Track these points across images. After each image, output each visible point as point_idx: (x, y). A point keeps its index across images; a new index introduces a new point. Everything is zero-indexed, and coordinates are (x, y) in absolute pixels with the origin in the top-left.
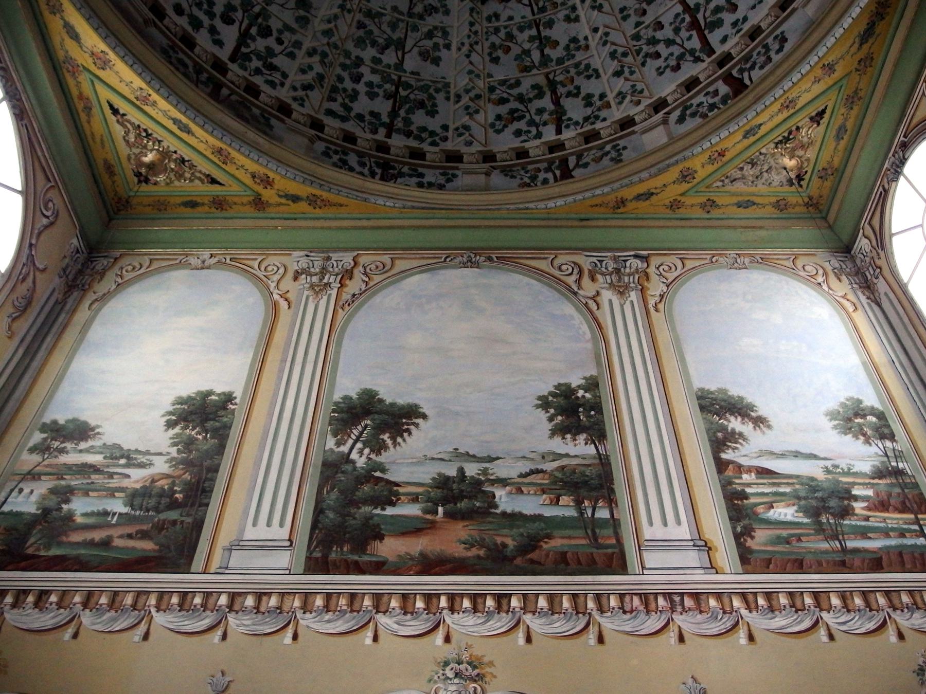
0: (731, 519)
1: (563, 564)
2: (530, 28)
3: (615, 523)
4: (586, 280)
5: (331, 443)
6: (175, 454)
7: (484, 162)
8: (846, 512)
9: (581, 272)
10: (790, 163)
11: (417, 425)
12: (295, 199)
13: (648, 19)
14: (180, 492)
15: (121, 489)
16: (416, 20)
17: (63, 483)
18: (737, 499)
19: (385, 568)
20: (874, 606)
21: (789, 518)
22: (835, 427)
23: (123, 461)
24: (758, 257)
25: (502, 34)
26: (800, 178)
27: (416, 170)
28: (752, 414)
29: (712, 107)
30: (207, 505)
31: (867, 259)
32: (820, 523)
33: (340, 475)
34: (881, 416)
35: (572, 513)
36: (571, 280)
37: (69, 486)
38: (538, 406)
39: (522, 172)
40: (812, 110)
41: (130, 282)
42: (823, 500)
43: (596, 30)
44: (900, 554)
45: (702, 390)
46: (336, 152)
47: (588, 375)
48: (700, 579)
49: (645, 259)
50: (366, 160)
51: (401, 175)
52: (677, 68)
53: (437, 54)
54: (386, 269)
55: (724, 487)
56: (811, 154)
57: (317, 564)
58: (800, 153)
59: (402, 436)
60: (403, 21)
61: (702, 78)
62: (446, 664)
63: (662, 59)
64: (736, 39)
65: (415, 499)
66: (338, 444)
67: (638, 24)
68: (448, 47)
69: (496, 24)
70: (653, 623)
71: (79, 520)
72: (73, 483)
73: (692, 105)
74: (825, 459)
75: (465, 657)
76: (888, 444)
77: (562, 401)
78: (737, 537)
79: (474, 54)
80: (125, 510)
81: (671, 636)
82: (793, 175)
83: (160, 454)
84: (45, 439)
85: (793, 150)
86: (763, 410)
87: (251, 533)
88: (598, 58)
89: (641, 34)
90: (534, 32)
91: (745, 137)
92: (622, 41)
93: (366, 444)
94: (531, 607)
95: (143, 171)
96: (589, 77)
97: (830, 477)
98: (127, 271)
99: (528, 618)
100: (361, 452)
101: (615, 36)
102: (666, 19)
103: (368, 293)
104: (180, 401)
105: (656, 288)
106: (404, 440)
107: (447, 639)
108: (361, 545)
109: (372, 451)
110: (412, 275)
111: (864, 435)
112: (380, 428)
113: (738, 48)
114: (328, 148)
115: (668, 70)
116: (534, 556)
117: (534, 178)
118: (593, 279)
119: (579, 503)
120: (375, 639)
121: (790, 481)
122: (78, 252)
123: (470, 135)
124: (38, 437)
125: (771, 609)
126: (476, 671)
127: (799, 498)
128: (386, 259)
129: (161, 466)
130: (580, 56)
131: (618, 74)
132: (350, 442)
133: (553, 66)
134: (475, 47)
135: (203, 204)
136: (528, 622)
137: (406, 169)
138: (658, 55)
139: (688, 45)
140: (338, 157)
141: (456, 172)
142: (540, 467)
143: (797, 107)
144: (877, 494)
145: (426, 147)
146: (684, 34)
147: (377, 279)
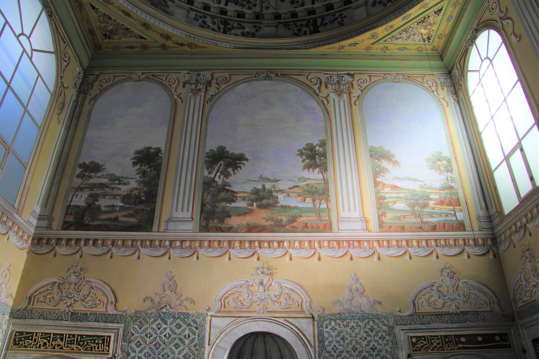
0: (377, 208)
1: (306, 228)
3: (328, 210)
4: (323, 88)
5: (206, 173)
6: (139, 179)
7: (275, 19)
8: (425, 206)
9: (321, 83)
10: (423, 31)
11: (244, 164)
12: (182, 45)
14: (143, 196)
15: (119, 195)
17: (94, 192)
18: (381, 199)
19: (232, 230)
20: (429, 245)
21: (402, 208)
22: (428, 166)
23: (117, 182)
24: (406, 76)
26: (429, 38)
27: (240, 25)
28: (393, 159)
30: (155, 202)
31: (457, 80)
32: (414, 210)
33: (211, 188)
34: (449, 161)
35: (311, 205)
36: (316, 87)
37: (96, 194)
38: (298, 155)
39: (294, 26)
40: (436, 8)
41: (106, 89)
42: (417, 200)
44: (444, 224)
45: (372, 147)
46: (201, 17)
47: (321, 139)
48: (362, 235)
49: (352, 76)
50: (215, 20)
51: (233, 28)
54: (228, 80)
55: (376, 194)
56: (435, 28)
57: (204, 228)
58: (429, 27)
59: (237, 169)
62: (258, 269)
65: (244, 199)
66: (209, 173)
70: (341, 252)
71: (104, 209)
72: (98, 192)
74: (421, 181)
75: (266, 266)
76: (449, 174)
77: (309, 152)
78: (379, 216)
80: (121, 204)
81: (348, 257)
82: (425, 37)
83: (132, 178)
84: (82, 171)
85: (426, 26)
86: (398, 158)
87: (175, 215)
91: (403, 20)
93: (221, 173)
94: (292, 246)
95: (108, 33)
97: (422, 190)
98: (103, 83)
99: (290, 251)
100: (219, 177)
103: (219, 94)
104: (138, 152)
105: (356, 92)
106: (238, 171)
107: (258, 259)
108: (222, 221)
109: (224, 176)
110: (239, 84)
111: (440, 170)
112: (228, 165)
114: (196, 15)
116: (294, 224)
117: (300, 30)
118: (326, 87)
119: (314, 201)
120: (230, 259)
121: (405, 191)
122: (79, 74)
123: (268, 3)
124: (78, 171)
125: (389, 247)
126: (270, 271)
127: (407, 199)
128: (227, 75)
129: (133, 184)
132: (215, 172)
135: (137, 47)
136: (291, 252)
137: (235, 24)
140: (201, 20)
141: (261, 25)
142: (298, 185)
143: (429, 7)
144: (440, 197)
145: (246, 11)
147: (223, 86)
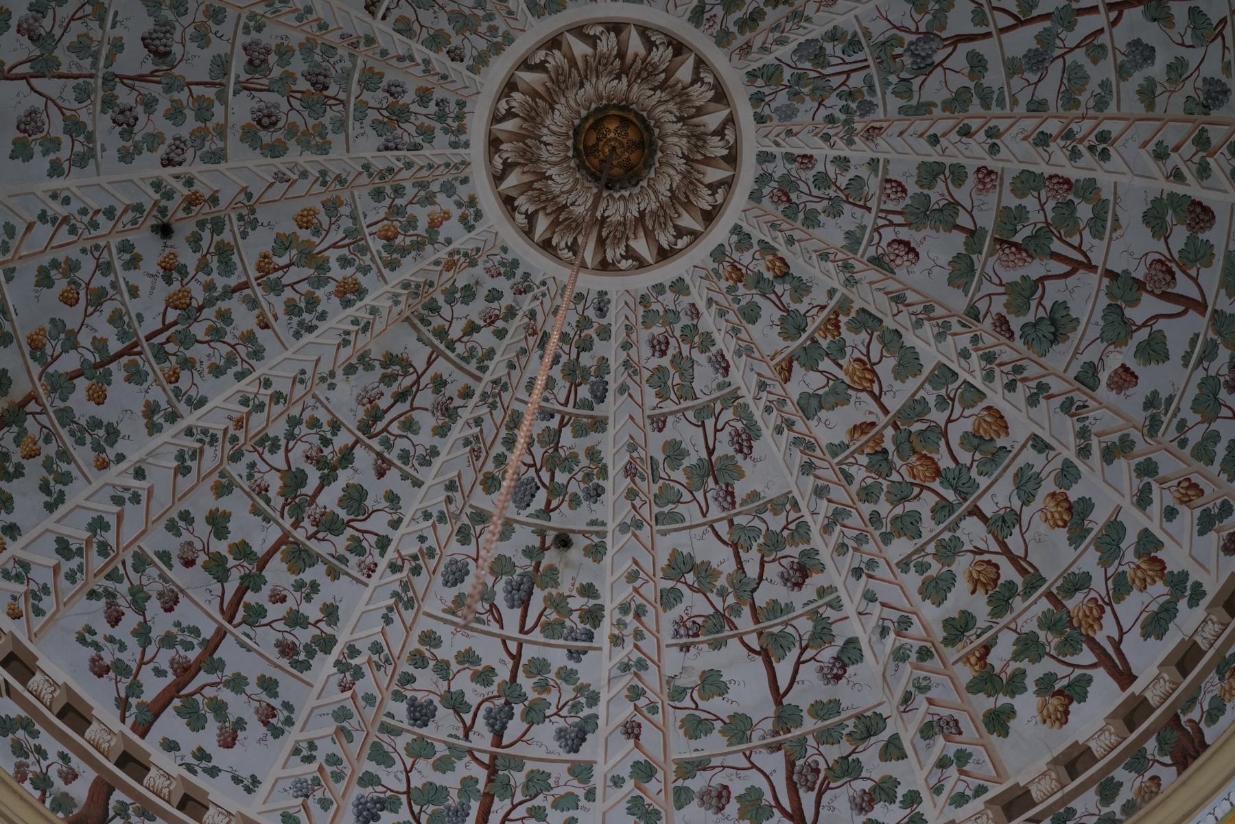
2: (122, 337)
13: (179, 575)
16: (100, 93)
25: (100, 281)
29: (42, 782)
43: (140, 474)
52: (99, 669)
53: (37, 149)
60: (94, 65)
61: (93, 731)
63: (109, 631)
64: (176, 770)
67: (165, 556)
68: (56, 170)
69: (117, 264)
73: (35, 735)
79: (49, 229)
88: (88, 494)
89: (152, 571)
90: (115, 346)
92: (128, 534)
96: (45, 488)
101: (134, 515)
102: (185, 612)
113: (161, 782)
115: (91, 652)
130: (84, 455)
131: (64, 548)
133: (53, 403)
134: (65, 228)
138: (115, 620)
139: (146, 675)
146: (164, 658)
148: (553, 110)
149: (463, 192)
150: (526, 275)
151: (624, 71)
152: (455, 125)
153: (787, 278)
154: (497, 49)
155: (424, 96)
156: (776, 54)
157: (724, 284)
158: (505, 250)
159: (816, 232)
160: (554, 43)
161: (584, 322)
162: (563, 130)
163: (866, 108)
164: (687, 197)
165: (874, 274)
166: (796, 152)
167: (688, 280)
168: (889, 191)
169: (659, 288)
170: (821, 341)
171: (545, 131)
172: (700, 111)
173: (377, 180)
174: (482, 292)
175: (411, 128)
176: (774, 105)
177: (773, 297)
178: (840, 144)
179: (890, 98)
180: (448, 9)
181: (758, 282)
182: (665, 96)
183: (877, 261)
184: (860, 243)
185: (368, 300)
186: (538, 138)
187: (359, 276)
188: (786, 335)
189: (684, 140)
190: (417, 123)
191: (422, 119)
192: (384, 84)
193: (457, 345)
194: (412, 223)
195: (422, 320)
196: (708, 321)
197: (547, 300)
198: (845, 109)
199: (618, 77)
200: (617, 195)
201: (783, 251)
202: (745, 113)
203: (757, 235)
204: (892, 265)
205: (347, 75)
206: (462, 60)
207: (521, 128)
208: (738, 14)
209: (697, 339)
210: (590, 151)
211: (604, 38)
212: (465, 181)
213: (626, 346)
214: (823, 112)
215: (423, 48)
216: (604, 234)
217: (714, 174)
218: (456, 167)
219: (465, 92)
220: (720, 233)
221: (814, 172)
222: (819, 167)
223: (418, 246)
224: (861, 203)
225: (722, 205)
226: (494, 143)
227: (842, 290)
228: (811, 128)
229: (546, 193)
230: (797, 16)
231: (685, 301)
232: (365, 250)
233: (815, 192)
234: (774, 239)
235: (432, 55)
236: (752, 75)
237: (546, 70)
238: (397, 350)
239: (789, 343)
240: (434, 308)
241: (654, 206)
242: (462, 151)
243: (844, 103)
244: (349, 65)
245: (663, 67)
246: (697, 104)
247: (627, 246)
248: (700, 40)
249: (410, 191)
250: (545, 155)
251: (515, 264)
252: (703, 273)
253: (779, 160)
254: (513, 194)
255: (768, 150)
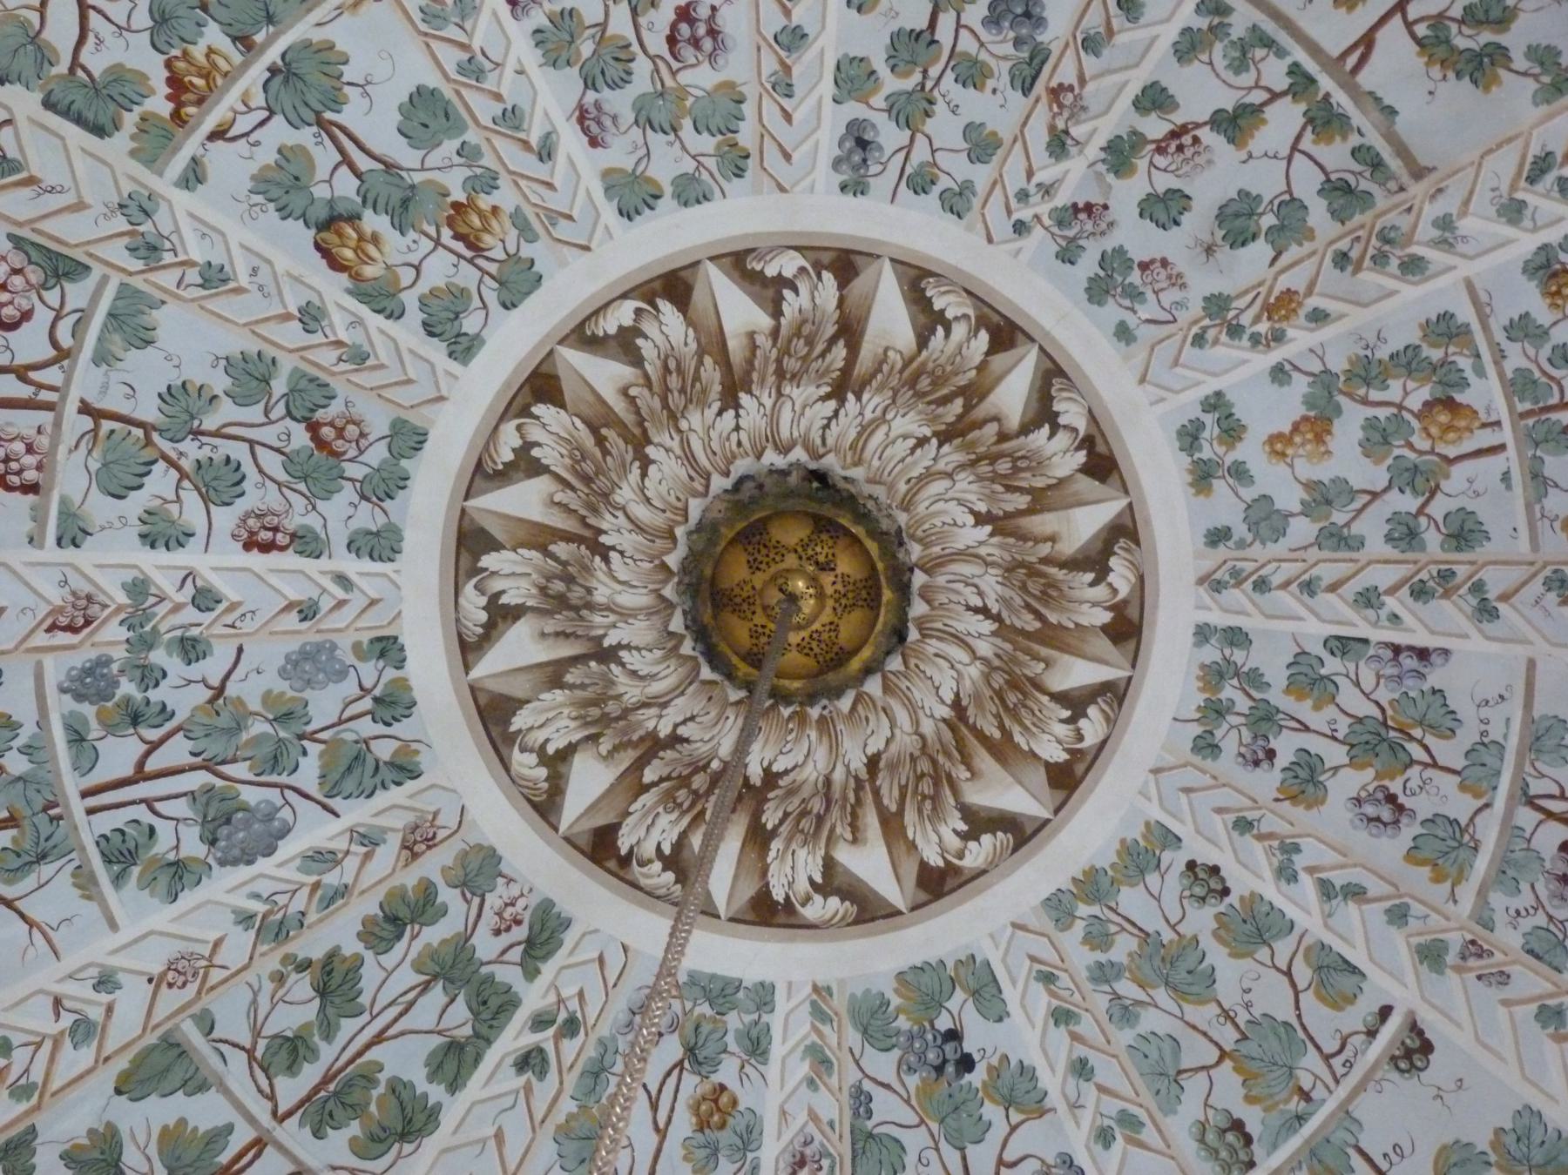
148: (957, 705)
149: (1225, 506)
150: (1068, 255)
151: (755, 795)
152: (1229, 692)
153: (321, 213)
154: (1092, 885)
155: (1305, 782)
156: (336, 826)
157: (505, 197)
158: (1124, 333)
159: (237, 343)
160: (937, 884)
161: (912, 111)
162: (933, 645)
163: (90, 683)
164: (601, 441)
165: (71, 232)
166: (289, 560)
167: (609, 213)
168: (30, 460)
169: (691, 192)
170: (223, 43)
171: (984, 648)
172: (554, 674)
173: (1462, 571)
174: (1198, 222)
175: (1350, 698)
176: (350, 687)
177: (364, 164)
178: (166, 583)
179: (25, 712)
180: (1213, 1009)
181: (405, 203)
182: (649, 720)
183: (61, 268)
184: (111, 315)
185: (1526, 244)
186: (1004, 630)
187: (1542, 313)
188: (327, 57)
189: (600, 596)
190: (1330, 711)
191: (1317, 720)
192: (1410, 830)
193: (1281, 82)
194: (1377, 439)
195: (1376, 164)
196: (551, 97)
197: (1015, 179)
198: (150, 676)
199: (771, 778)
200: (799, 454)
201: (332, 288)
202: (429, 667)
203: (408, 332)
204: (17, 260)
205: (1505, 873)
206: (1191, 865)
207: (1048, 663)
208: (434, 935)
209: (587, 49)
210: (866, 594)
211: (803, 886)
212: (1218, 536)
213: (793, 39)
214: (213, 668)
215: (1291, 912)
216: (840, 351)
217: (525, 500)
218: (1238, 578)
219: (1191, 777)
220: (512, 340)
221: (241, 506)
222: (225, 518)
223: (1366, 372)
224: (107, 425)
225: (503, 418)
226: (1126, 629)
227: (164, 184)
228: (248, 626)
229: (996, 478)
230: (274, 928)
231: (619, 153)
232: (1518, 385)
233: (239, 452)
234: (357, 322)
235: (1271, 891)
236: (404, 769)
237: (967, 812)
238: (1460, 90)
239: (317, 36)
240: (1340, 193)
241: (694, 420)
242: (1218, 619)
243: (154, 695)
244: (1498, 900)
245: (647, 799)
246: (559, 695)
247: (777, 313)
248: (539, 865)
249: (1372, 527)
250: (991, 583)
251: (1098, 291)
252: (563, 230)
253: (339, 539)
254: (1087, 484)
255: (367, 565)
